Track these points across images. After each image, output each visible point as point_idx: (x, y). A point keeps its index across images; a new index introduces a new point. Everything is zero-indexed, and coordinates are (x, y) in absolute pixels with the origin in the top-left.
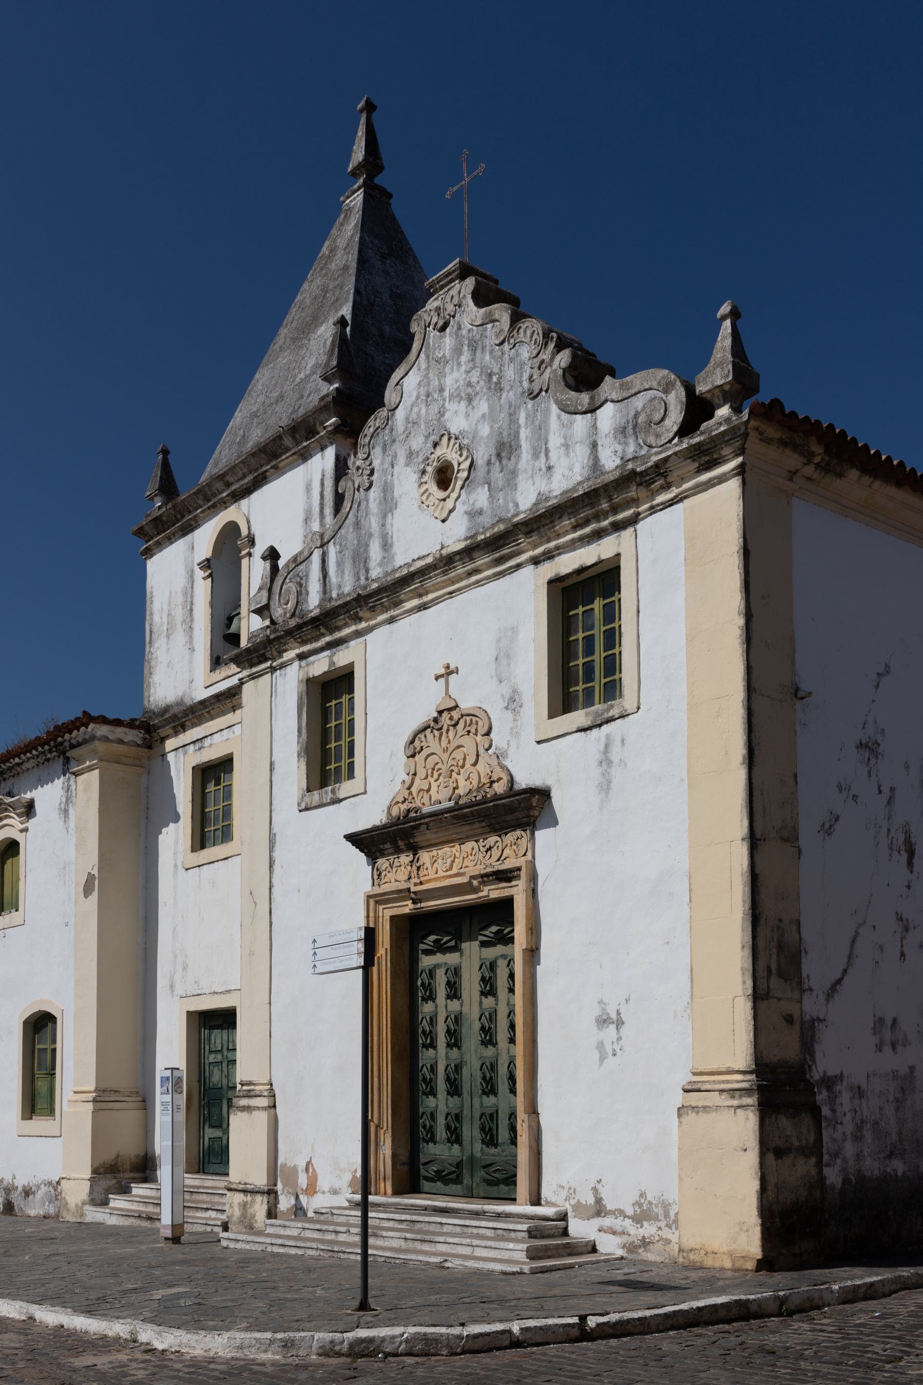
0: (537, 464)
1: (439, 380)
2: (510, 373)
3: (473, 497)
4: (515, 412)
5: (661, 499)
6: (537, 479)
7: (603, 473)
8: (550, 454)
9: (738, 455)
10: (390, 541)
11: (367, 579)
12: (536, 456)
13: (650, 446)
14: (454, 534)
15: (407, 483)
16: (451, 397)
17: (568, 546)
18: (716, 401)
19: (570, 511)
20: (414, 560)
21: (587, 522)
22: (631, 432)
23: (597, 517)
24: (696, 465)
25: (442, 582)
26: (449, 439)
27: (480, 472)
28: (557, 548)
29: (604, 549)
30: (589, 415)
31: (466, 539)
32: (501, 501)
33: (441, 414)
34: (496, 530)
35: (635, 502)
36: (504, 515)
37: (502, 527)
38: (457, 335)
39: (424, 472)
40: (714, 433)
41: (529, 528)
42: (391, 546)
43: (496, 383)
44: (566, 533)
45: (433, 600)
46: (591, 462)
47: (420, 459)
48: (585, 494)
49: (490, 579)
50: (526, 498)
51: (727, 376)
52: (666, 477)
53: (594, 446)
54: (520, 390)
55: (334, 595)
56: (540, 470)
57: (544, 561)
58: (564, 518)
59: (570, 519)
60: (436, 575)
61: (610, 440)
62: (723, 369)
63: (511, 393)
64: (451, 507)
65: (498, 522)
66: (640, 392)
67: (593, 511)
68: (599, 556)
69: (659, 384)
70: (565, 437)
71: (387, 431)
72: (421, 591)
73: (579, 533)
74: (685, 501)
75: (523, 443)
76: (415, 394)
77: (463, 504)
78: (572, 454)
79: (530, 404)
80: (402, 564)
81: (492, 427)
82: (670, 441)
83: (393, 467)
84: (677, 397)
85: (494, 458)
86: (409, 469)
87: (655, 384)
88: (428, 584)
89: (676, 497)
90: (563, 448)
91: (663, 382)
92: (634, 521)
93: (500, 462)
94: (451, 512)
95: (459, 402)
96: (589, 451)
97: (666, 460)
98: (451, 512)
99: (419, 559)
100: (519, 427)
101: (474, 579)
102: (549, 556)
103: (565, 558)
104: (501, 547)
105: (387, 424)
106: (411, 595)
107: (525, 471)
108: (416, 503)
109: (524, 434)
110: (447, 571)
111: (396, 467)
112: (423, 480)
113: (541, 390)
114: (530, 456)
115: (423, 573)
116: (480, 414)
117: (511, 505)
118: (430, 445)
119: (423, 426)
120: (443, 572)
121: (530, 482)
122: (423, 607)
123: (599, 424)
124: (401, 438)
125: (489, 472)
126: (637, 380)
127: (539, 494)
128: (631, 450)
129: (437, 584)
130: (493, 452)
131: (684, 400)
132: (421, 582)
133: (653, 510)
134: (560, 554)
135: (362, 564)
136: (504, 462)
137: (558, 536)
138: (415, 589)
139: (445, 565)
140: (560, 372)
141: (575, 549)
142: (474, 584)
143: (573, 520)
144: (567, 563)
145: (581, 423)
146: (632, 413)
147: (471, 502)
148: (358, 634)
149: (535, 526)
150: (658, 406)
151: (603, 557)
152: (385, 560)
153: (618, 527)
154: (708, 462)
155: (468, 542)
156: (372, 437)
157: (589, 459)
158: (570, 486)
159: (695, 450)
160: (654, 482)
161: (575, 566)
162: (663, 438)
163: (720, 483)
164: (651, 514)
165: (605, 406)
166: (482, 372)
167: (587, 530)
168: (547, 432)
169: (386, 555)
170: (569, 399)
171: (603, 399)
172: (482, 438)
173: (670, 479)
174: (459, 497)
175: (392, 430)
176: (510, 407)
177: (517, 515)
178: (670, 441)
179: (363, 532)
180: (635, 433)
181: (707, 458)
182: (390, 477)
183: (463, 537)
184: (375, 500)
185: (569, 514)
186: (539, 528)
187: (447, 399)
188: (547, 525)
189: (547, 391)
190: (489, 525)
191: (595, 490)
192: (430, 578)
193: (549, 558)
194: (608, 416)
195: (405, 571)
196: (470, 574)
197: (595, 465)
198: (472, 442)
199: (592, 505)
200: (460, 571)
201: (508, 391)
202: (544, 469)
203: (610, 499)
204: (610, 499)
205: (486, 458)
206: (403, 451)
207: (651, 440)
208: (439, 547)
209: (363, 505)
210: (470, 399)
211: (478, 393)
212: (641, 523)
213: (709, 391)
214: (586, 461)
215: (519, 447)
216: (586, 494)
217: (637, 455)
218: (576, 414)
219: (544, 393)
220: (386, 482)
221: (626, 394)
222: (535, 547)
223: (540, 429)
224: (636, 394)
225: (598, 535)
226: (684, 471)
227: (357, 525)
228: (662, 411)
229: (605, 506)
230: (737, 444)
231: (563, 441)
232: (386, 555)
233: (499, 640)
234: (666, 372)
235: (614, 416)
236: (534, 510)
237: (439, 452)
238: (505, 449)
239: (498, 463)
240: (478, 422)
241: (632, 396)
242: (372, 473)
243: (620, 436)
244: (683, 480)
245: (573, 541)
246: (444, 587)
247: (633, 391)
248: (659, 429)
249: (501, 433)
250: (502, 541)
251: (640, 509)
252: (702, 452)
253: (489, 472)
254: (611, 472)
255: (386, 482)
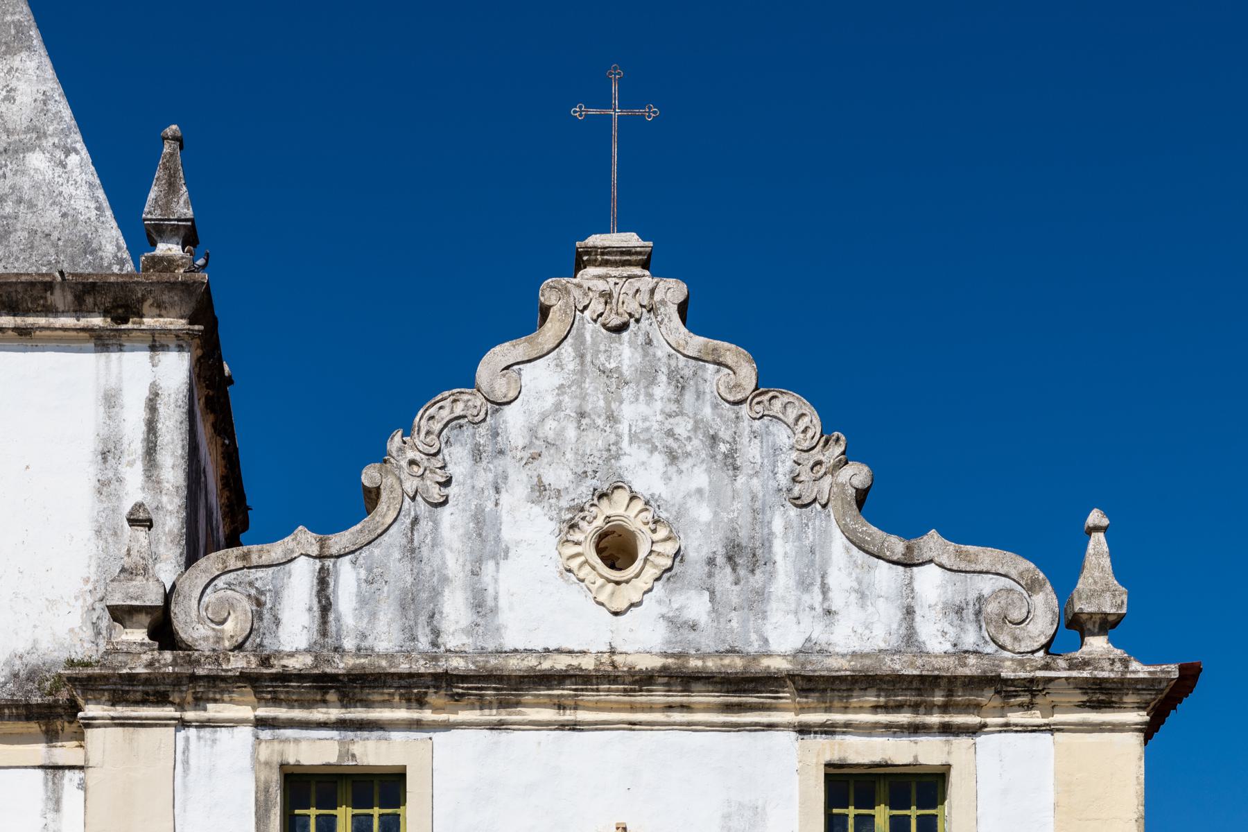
0: (806, 598)
1: (608, 403)
2: (752, 452)
3: (678, 600)
4: (763, 512)
5: (1015, 717)
6: (806, 618)
7: (922, 653)
8: (831, 594)
9: (1140, 708)
10: (490, 603)
11: (434, 644)
12: (804, 585)
13: (1003, 647)
14: (642, 640)
15: (530, 531)
16: (633, 438)
17: (864, 728)
18: (1090, 626)
19: (885, 686)
20: (547, 650)
21: (898, 708)
22: (972, 617)
23: (915, 708)
24: (1085, 698)
25: (616, 702)
26: (633, 498)
27: (695, 568)
28: (847, 725)
29: (927, 752)
30: (901, 568)
31: (665, 655)
32: (734, 624)
33: (613, 454)
34: (727, 661)
35: (977, 708)
36: (739, 645)
37: (735, 664)
38: (646, 354)
39: (573, 526)
40: (1129, 676)
41: (811, 685)
42: (494, 611)
43: (726, 456)
44: (860, 709)
45: (596, 723)
46: (903, 631)
47: (564, 503)
48: (921, 676)
49: (712, 726)
50: (782, 638)
51: (1120, 606)
52: (1034, 696)
53: (909, 612)
54: (772, 484)
55: (349, 644)
56: (812, 608)
57: (816, 733)
58: (869, 692)
59: (878, 696)
60: (609, 690)
61: (935, 614)
62: (1114, 596)
63: (755, 481)
64: (636, 599)
65: (728, 651)
66: (987, 572)
67: (918, 699)
68: (916, 757)
69: (1021, 574)
70: (860, 583)
71: (482, 430)
72: (570, 702)
73: (883, 718)
74: (1057, 735)
75: (779, 558)
76: (550, 401)
77: (660, 602)
78: (870, 609)
79: (793, 512)
80: (521, 647)
81: (716, 514)
82: (1033, 652)
83: (497, 491)
84: (1046, 602)
85: (720, 560)
86: (537, 509)
87: (1014, 574)
88: (589, 697)
89: (1046, 725)
90: (854, 595)
91: (1027, 576)
92: (974, 731)
93: (734, 570)
94: (632, 605)
95: (651, 452)
96: (900, 615)
97: (1051, 680)
98: (632, 605)
99: (559, 651)
100: (771, 533)
101: (677, 717)
102: (828, 730)
103: (851, 740)
104: (745, 691)
105: (484, 420)
106: (547, 700)
107: (783, 599)
108: (552, 569)
109: (780, 548)
110: (635, 691)
111: (505, 498)
112: (570, 538)
113: (815, 500)
114: (792, 583)
115: (584, 679)
116: (693, 486)
117: (753, 637)
118: (585, 489)
119: (569, 456)
120: (625, 690)
121: (791, 617)
122: (574, 726)
123: (916, 585)
124: (519, 455)
125: (710, 575)
126: (987, 556)
127: (809, 640)
128: (970, 639)
129: (606, 702)
130: (721, 551)
131: (1057, 610)
132: (576, 690)
133: (1006, 727)
134: (844, 733)
135: (423, 619)
136: (742, 572)
137: (846, 709)
138: (562, 696)
139: (634, 683)
140: (852, 491)
141: (870, 735)
142: (681, 724)
143: (882, 699)
144: (863, 750)
145: (885, 576)
146: (972, 596)
147: (675, 606)
148: (417, 725)
149: (822, 687)
150: (1018, 603)
151: (922, 760)
152: (481, 630)
153: (947, 730)
154: (1099, 701)
155: (670, 661)
156: (446, 425)
157: (900, 625)
158: (866, 650)
159: (1094, 683)
160: (1015, 696)
161: (877, 759)
162: (1023, 644)
163: (1112, 731)
164: (1000, 732)
165: (927, 567)
166: (696, 429)
167: (904, 718)
168: (826, 562)
169: (479, 620)
170: (870, 535)
171: (926, 557)
172: (695, 521)
173: (1039, 700)
174: (650, 590)
175: (495, 434)
176: (754, 498)
177: (769, 655)
178: (1033, 652)
179: (428, 570)
180: (978, 621)
181: (1102, 697)
182: (490, 505)
183: (657, 650)
184: (453, 527)
185: (880, 690)
186: (824, 690)
187: (626, 438)
188: (839, 690)
189: (824, 506)
190: (712, 650)
191: (937, 677)
192: (598, 690)
193: (826, 733)
194: (930, 583)
195: (531, 662)
196: (669, 708)
197: (910, 637)
198: (676, 519)
199: (919, 691)
200: (659, 697)
201: (751, 476)
202: (819, 610)
203: (950, 693)
204: (950, 693)
205: (705, 552)
206: (524, 477)
207: (1005, 639)
208: (606, 648)
209: (425, 526)
210: (673, 457)
211: (688, 454)
212: (983, 736)
213: (1091, 614)
214: (895, 626)
215: (769, 562)
216: (922, 678)
217: (980, 649)
218: (879, 557)
219: (818, 506)
220: (480, 510)
221: (963, 566)
222: (802, 709)
223: (812, 552)
224: (981, 572)
225: (915, 729)
226: (1063, 699)
227: (412, 552)
228: (1024, 611)
229: (939, 699)
230: (1148, 697)
231: (855, 585)
232: (479, 620)
233: (727, 817)
234: (1032, 566)
235: (944, 586)
236: (801, 657)
237: (605, 509)
238: (742, 555)
239: (728, 570)
240: (689, 495)
241: (974, 572)
242: (447, 483)
243: (953, 616)
244: (1054, 708)
245: (876, 726)
246: (611, 710)
247: (978, 568)
248: (1017, 630)
249: (735, 529)
250: (752, 686)
251: (989, 720)
252: (1101, 689)
253: (710, 575)
254: (936, 657)
255: (480, 510)
